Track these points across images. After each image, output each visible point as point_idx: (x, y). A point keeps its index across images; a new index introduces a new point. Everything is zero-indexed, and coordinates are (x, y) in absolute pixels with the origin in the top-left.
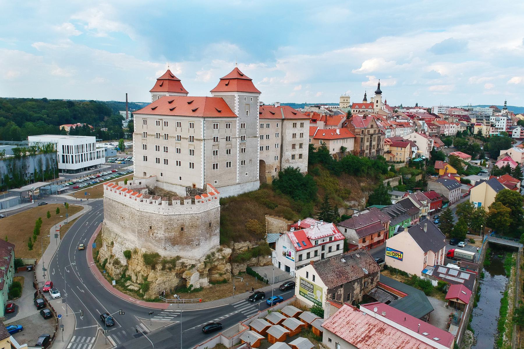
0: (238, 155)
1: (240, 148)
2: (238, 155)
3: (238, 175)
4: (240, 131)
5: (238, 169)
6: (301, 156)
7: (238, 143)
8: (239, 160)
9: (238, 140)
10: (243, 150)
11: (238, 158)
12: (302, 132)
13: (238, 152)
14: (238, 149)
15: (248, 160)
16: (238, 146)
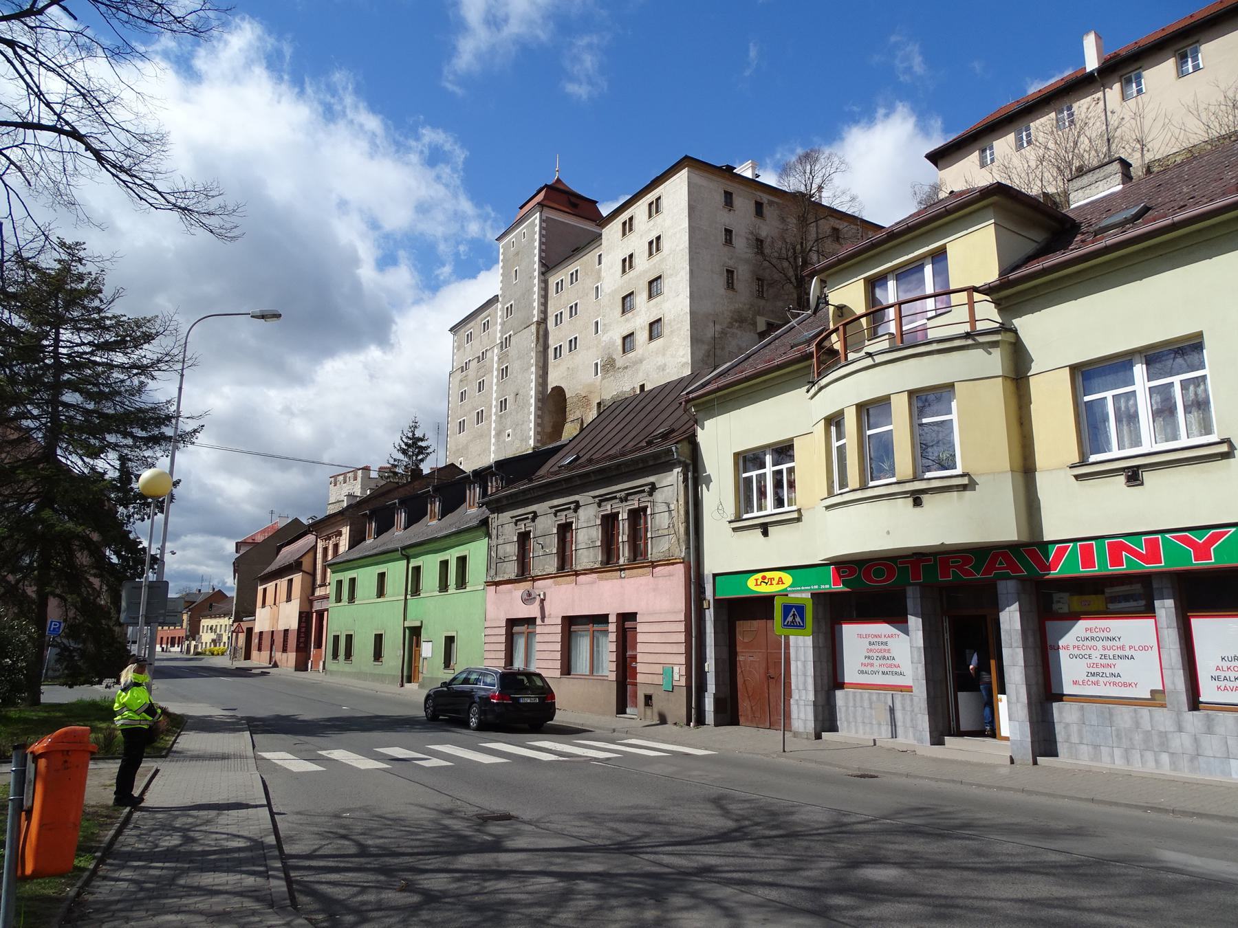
0: (495, 388)
1: (498, 370)
2: (495, 388)
3: (493, 440)
4: (503, 324)
5: (493, 425)
6: (655, 329)
7: (496, 359)
8: (496, 400)
9: (496, 351)
10: (504, 372)
11: (495, 395)
12: (653, 236)
13: (495, 380)
14: (495, 373)
15: (512, 395)
16: (495, 366)
